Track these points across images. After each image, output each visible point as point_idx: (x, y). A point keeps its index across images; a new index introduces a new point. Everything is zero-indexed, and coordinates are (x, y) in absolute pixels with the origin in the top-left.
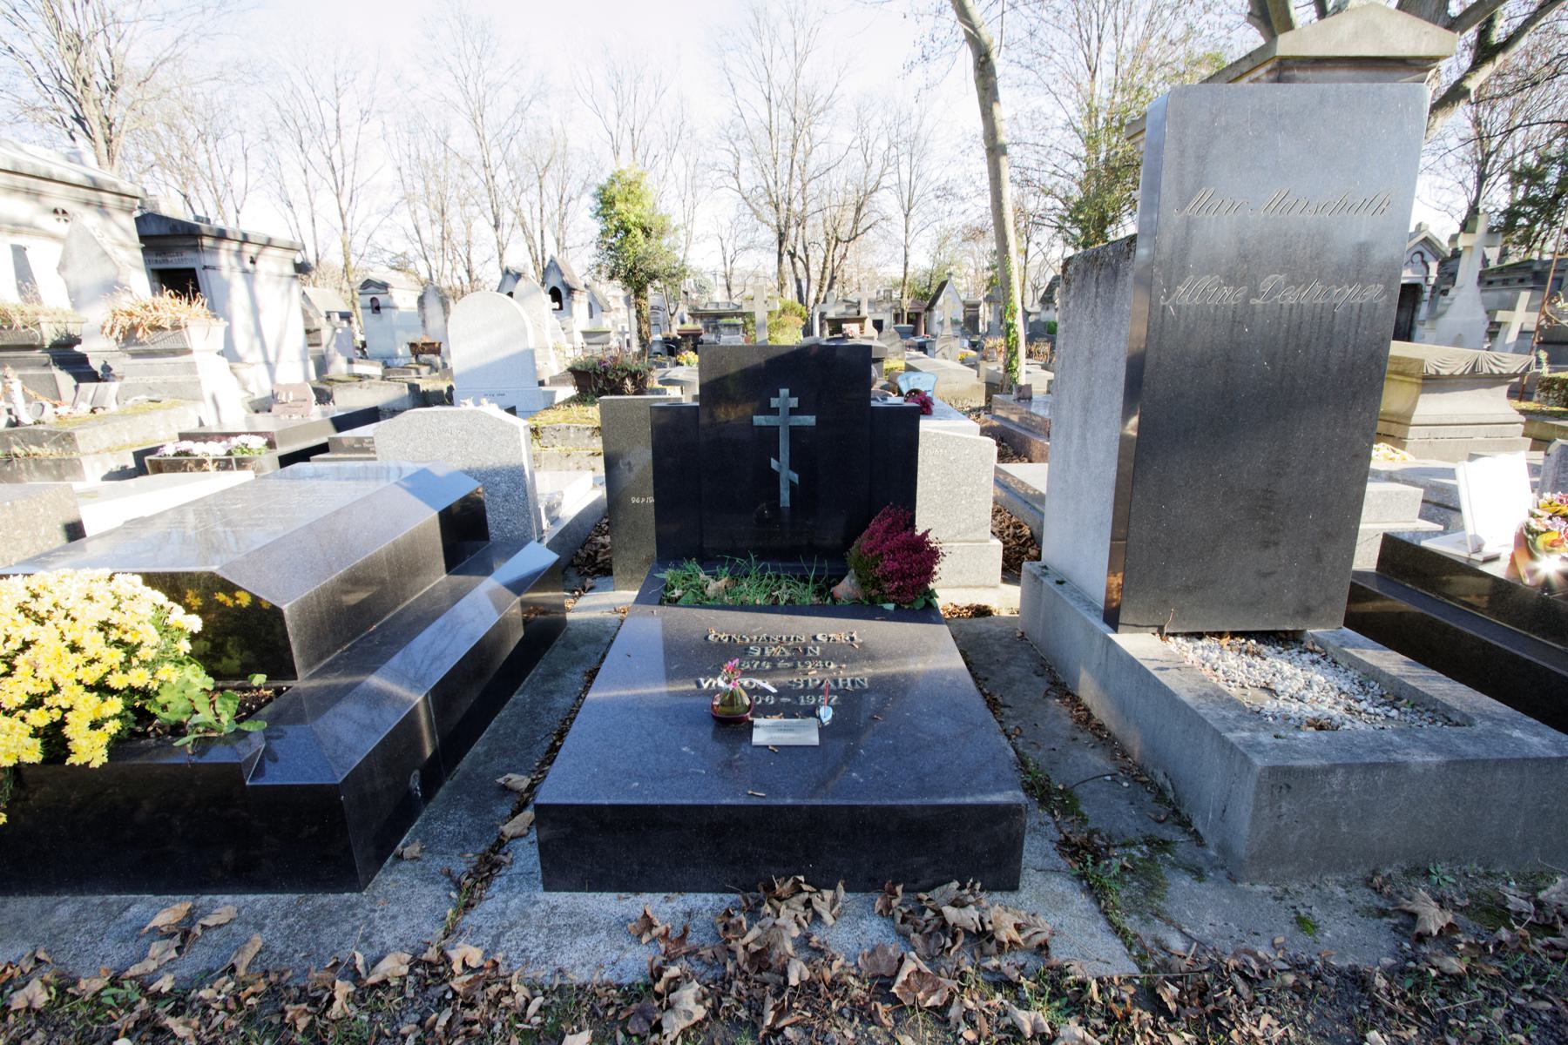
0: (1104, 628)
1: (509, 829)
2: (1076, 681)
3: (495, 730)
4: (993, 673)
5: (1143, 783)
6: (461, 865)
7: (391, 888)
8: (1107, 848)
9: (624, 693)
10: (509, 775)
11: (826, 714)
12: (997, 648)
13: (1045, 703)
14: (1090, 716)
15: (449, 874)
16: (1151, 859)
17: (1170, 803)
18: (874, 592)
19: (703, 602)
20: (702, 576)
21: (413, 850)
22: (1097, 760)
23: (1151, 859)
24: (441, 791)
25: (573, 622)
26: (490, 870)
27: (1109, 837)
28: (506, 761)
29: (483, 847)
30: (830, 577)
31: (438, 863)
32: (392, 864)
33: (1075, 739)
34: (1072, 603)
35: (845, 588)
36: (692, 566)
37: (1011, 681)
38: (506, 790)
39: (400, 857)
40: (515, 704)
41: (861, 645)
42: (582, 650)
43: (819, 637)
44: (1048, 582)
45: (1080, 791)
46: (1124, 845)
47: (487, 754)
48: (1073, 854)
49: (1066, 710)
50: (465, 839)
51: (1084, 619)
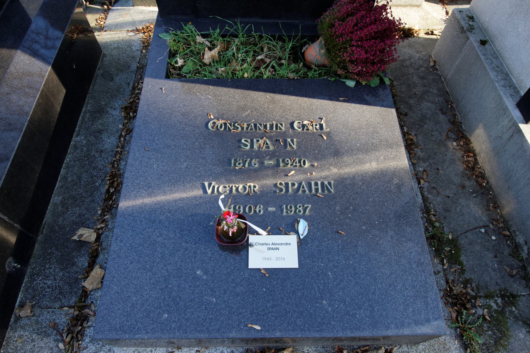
0: (517, 114)
1: (88, 284)
2: (472, 131)
3: (65, 178)
4: (410, 107)
5: (505, 236)
6: (63, 317)
7: (19, 344)
8: (475, 298)
9: (148, 200)
10: (81, 231)
11: (303, 227)
12: (415, 79)
13: (446, 146)
14: (476, 162)
15: (55, 327)
16: (502, 312)
17: (522, 260)
18: (340, 72)
19: (201, 76)
21: (25, 312)
22: (474, 210)
23: (502, 312)
24: (37, 246)
25: (107, 45)
26: (81, 325)
27: (478, 288)
28: (77, 210)
29: (73, 300)
30: (303, 37)
31: (46, 317)
32: (16, 321)
33: (463, 187)
34: (492, 75)
35: (314, 52)
36: (190, 27)
37: (423, 119)
38: (81, 244)
39: (19, 318)
40: (76, 147)
41: (328, 134)
42: (117, 79)
43: (296, 125)
44: (474, 39)
45: (462, 241)
46: (487, 297)
47: (63, 203)
48: (453, 305)
49: (459, 154)
50: (61, 293)
51: (501, 98)
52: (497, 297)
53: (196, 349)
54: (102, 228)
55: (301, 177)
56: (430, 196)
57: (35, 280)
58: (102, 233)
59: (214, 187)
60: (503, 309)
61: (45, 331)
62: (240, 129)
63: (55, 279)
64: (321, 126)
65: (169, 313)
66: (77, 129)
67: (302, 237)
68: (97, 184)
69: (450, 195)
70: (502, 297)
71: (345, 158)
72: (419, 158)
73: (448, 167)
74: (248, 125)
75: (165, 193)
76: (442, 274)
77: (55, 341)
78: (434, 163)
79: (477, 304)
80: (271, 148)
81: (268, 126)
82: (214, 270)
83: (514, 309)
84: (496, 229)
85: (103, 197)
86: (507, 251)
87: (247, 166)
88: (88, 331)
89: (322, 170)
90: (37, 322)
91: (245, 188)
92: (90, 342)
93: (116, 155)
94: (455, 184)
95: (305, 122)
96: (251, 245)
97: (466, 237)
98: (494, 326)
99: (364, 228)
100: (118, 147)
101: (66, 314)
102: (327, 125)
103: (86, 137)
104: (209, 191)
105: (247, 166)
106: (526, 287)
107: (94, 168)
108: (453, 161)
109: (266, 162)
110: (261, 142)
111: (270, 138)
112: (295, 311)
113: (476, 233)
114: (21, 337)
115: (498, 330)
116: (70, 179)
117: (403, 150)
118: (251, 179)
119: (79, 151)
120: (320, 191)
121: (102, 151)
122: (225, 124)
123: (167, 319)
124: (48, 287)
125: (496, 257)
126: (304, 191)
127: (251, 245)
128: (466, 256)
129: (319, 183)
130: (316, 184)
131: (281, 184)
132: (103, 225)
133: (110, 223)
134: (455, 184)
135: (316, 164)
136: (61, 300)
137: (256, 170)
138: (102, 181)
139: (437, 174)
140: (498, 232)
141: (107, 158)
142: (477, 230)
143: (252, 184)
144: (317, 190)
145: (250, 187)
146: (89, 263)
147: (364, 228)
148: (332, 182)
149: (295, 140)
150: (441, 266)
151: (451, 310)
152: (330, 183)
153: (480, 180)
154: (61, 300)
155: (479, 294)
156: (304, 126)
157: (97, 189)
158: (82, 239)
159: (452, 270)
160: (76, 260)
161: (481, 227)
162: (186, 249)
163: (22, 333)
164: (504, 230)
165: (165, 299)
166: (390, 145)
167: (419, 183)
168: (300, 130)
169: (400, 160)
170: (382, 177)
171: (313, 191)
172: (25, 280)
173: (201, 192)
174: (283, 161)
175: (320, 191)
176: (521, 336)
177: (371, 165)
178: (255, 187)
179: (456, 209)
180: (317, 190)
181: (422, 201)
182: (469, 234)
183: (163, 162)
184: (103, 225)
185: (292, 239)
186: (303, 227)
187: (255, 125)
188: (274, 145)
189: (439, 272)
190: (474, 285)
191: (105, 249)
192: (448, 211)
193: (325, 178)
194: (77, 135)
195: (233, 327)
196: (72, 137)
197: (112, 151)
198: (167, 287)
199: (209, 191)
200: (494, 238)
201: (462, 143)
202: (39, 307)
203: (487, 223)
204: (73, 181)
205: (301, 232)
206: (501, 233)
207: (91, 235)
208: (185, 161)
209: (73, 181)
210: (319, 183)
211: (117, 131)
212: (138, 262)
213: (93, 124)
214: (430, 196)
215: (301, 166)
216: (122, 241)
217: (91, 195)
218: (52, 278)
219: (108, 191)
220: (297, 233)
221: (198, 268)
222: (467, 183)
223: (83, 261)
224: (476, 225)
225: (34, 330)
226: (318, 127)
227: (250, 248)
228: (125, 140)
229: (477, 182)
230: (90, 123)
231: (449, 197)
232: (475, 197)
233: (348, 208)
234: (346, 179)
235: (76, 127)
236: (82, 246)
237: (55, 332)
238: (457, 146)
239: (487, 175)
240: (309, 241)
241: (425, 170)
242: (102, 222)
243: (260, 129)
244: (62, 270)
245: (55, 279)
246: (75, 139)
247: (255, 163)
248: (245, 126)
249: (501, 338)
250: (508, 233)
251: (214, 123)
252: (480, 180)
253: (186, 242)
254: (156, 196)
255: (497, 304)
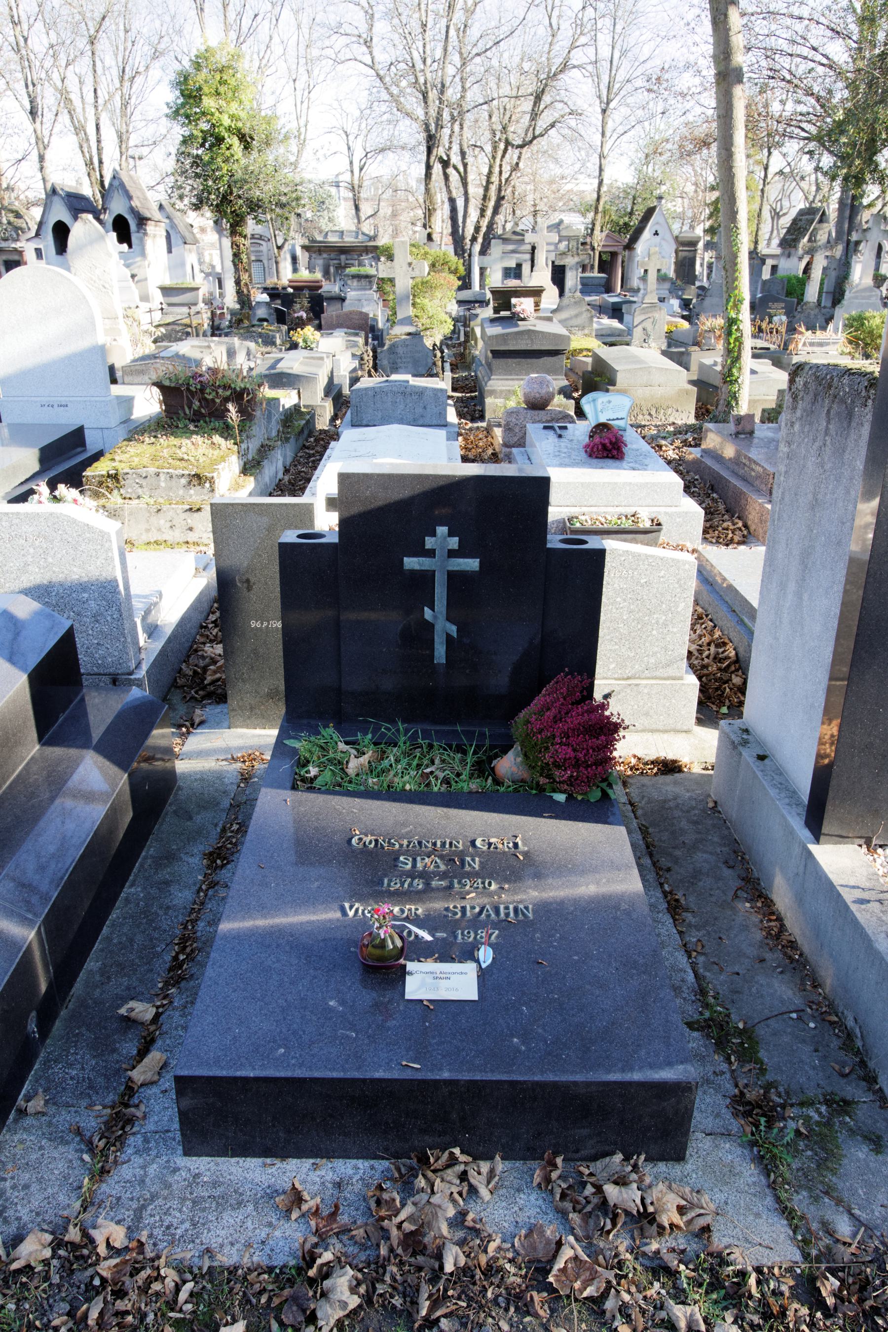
0: (805, 834)
1: (138, 1075)
2: (771, 885)
3: (108, 939)
4: (676, 861)
5: (832, 1023)
6: (91, 1121)
7: (19, 1150)
8: (783, 1106)
9: (261, 923)
10: (132, 1004)
11: (486, 955)
12: (684, 824)
13: (733, 908)
14: (782, 928)
15: (78, 1132)
16: (828, 1124)
17: (858, 1053)
18: (542, 780)
19: (343, 786)
20: (342, 746)
21: (37, 1104)
22: (782, 991)
23: (828, 1124)
24: (58, 1023)
25: (186, 776)
26: (123, 1128)
27: (787, 1093)
28: (125, 981)
29: (111, 1098)
30: (492, 747)
31: (65, 1118)
32: (16, 1121)
33: (762, 961)
34: (773, 792)
35: (509, 764)
36: (329, 732)
37: (697, 874)
38: (129, 1022)
39: (22, 1113)
40: (127, 901)
41: (526, 854)
42: (198, 819)
43: (478, 843)
44: (748, 755)
45: (762, 1031)
46: (802, 1104)
47: (103, 971)
48: (747, 1114)
49: (756, 918)
50: (90, 1087)
51: (783, 816)
52: (820, 1103)
53: (312, 1161)
54: (163, 1006)
55: (485, 900)
56: (708, 974)
57: (50, 1067)
58: (162, 1013)
59: (357, 910)
60: (829, 1119)
61: (62, 1137)
62: (397, 846)
63: (83, 1069)
64: (516, 845)
65: (286, 1047)
66: (131, 878)
67: (484, 966)
68: (159, 949)
69: (741, 972)
70: (828, 1103)
71: (550, 881)
72: (690, 925)
73: (736, 936)
74: (409, 843)
75: (286, 915)
76: (728, 1076)
77: (76, 1151)
78: (715, 932)
79: (787, 1115)
80: (443, 867)
81: (439, 844)
82: (354, 1001)
83: (847, 1119)
84: (816, 1014)
85: (168, 965)
86: (835, 1043)
87: (406, 886)
88: (131, 1140)
89: (516, 893)
90: (50, 1124)
91: (402, 911)
92: (136, 1153)
93: (191, 913)
94: (748, 957)
95: (492, 840)
96: (410, 973)
97: (768, 1026)
98: (816, 1143)
99: (576, 958)
100: (195, 903)
101: (97, 1117)
102: (524, 844)
103: (145, 888)
104: (351, 913)
105: (406, 886)
106: (869, 1090)
107: (155, 929)
108: (745, 928)
109: (434, 883)
110: (427, 860)
111: (441, 857)
112: (471, 1050)
113: (784, 1020)
114: (22, 1142)
115: (823, 1149)
116: (115, 941)
117: (636, 872)
118: (411, 901)
119: (132, 906)
120: (512, 915)
121: (168, 908)
122: (376, 841)
123: (283, 1055)
124: (72, 1078)
125: (816, 1051)
126: (489, 916)
127: (410, 973)
128: (767, 1050)
129: (511, 907)
130: (507, 908)
131: (455, 907)
132: (165, 1002)
133: (176, 1000)
134: (748, 957)
135: (506, 886)
136: (90, 1097)
137: (419, 892)
138: (167, 945)
139: (719, 945)
140: (821, 1018)
141: (176, 917)
142: (785, 1016)
143: (413, 907)
144: (507, 915)
145: (410, 910)
146: (139, 1051)
147: (576, 958)
148: (530, 907)
149: (477, 859)
150: (726, 1065)
151: (743, 1122)
152: (527, 908)
153: (789, 951)
154: (90, 1097)
155: (789, 1101)
156: (490, 844)
157: (159, 955)
158: (133, 1014)
159: (745, 1069)
160: (118, 1045)
161: (791, 1012)
162: (315, 977)
163: (25, 1136)
164: (830, 1014)
165: (281, 1032)
166: (614, 866)
167: (689, 957)
168: (485, 848)
169: (630, 883)
170: (607, 909)
171: (502, 915)
172: (36, 1067)
173: (338, 915)
174: (459, 882)
175: (512, 915)
176: (861, 1155)
177: (588, 888)
178: (417, 909)
179: (750, 989)
180: (507, 915)
181: (694, 980)
182: (771, 1022)
183: (284, 881)
184: (165, 1002)
185: (470, 968)
186: (486, 955)
187: (420, 843)
188: (447, 865)
189: (724, 1073)
190: (781, 1089)
191: (166, 1033)
192: (737, 992)
193: (521, 902)
194: (132, 886)
195: (380, 1066)
196: (123, 887)
197: (185, 908)
198: (285, 1019)
199: (351, 913)
200: (812, 1025)
201: (759, 904)
202: (55, 1104)
203: (802, 1007)
204: (120, 943)
205: (481, 958)
206: (824, 1020)
207: (146, 1011)
208: (317, 880)
209: (120, 943)
210: (511, 907)
211: (195, 884)
212: (245, 990)
213: (156, 873)
214: (708, 974)
215: (484, 887)
216: (221, 966)
217: (149, 963)
218: (79, 1066)
219: (175, 958)
220: (477, 961)
221: (331, 998)
222: (768, 956)
223: (130, 1048)
224: (784, 1009)
225: (43, 1134)
226: (511, 845)
227: (408, 978)
228: (206, 895)
229: (785, 954)
230: (152, 871)
231: (738, 974)
232: (782, 972)
233: (553, 936)
234: (551, 903)
235: (129, 875)
236: (129, 1028)
237: (78, 1139)
238: (752, 907)
239: (799, 942)
240: (495, 971)
241: (699, 940)
242: (164, 998)
243: (426, 847)
244: (95, 1057)
245: (83, 1069)
246: (127, 891)
247: (419, 884)
248: (405, 842)
249: (826, 1159)
250: (836, 1019)
251: (360, 839)
252: (789, 951)
253: (315, 969)
254: (273, 917)
255: (820, 1114)
